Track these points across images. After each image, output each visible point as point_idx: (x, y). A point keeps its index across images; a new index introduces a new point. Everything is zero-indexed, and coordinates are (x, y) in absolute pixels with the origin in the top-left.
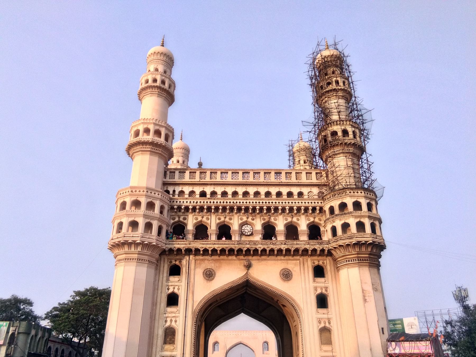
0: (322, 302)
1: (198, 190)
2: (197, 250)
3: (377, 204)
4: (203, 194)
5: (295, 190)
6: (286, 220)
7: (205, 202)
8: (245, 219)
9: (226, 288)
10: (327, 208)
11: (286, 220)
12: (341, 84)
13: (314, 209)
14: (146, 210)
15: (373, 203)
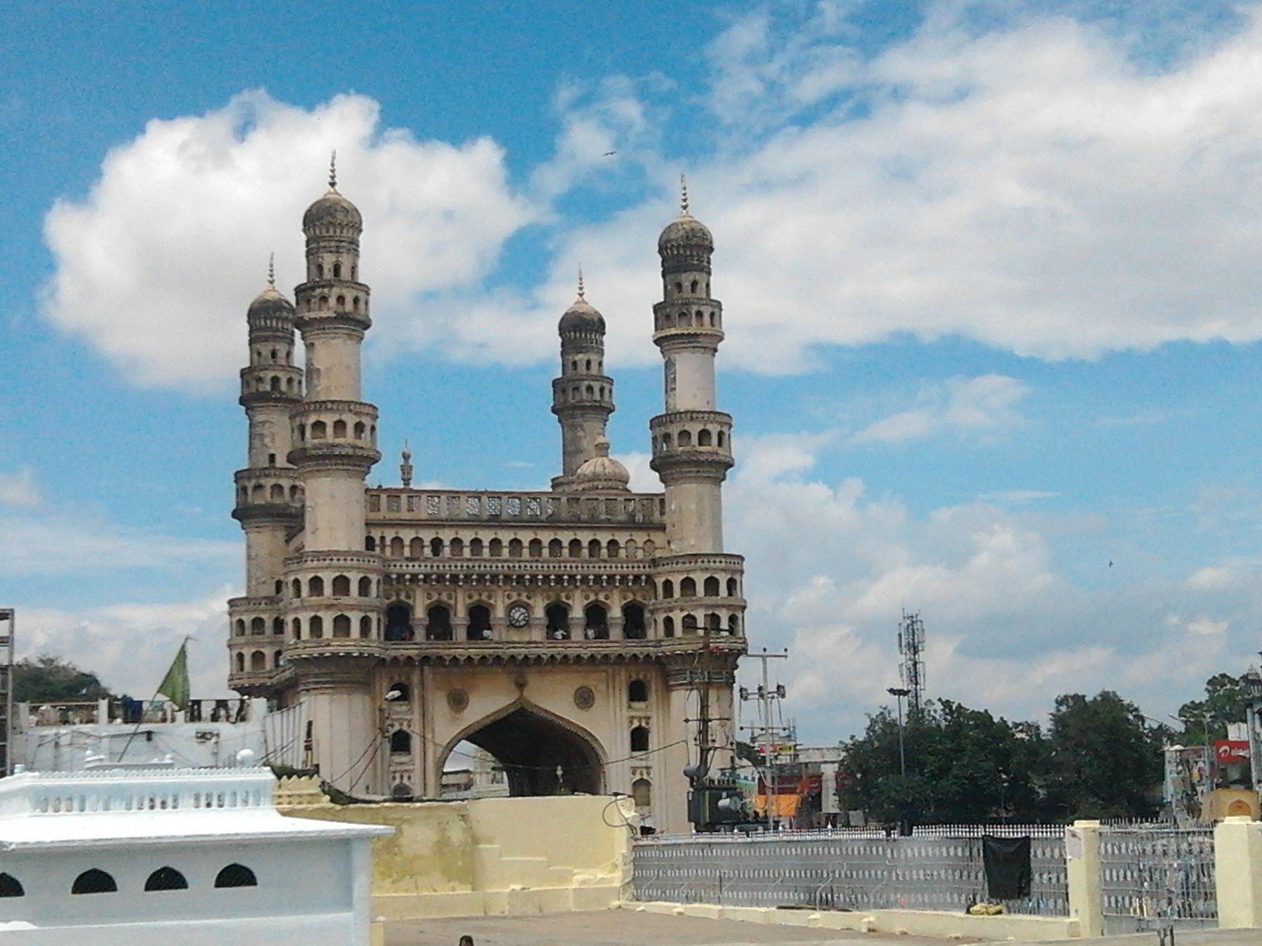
0: (639, 740)
1: (427, 536)
2: (440, 658)
3: (742, 572)
4: (437, 544)
5: (604, 538)
6: (587, 597)
7: (448, 569)
8: (515, 598)
9: (488, 721)
10: (660, 581)
11: (587, 597)
12: (706, 317)
13: (637, 578)
14: (360, 594)
15: (737, 577)
